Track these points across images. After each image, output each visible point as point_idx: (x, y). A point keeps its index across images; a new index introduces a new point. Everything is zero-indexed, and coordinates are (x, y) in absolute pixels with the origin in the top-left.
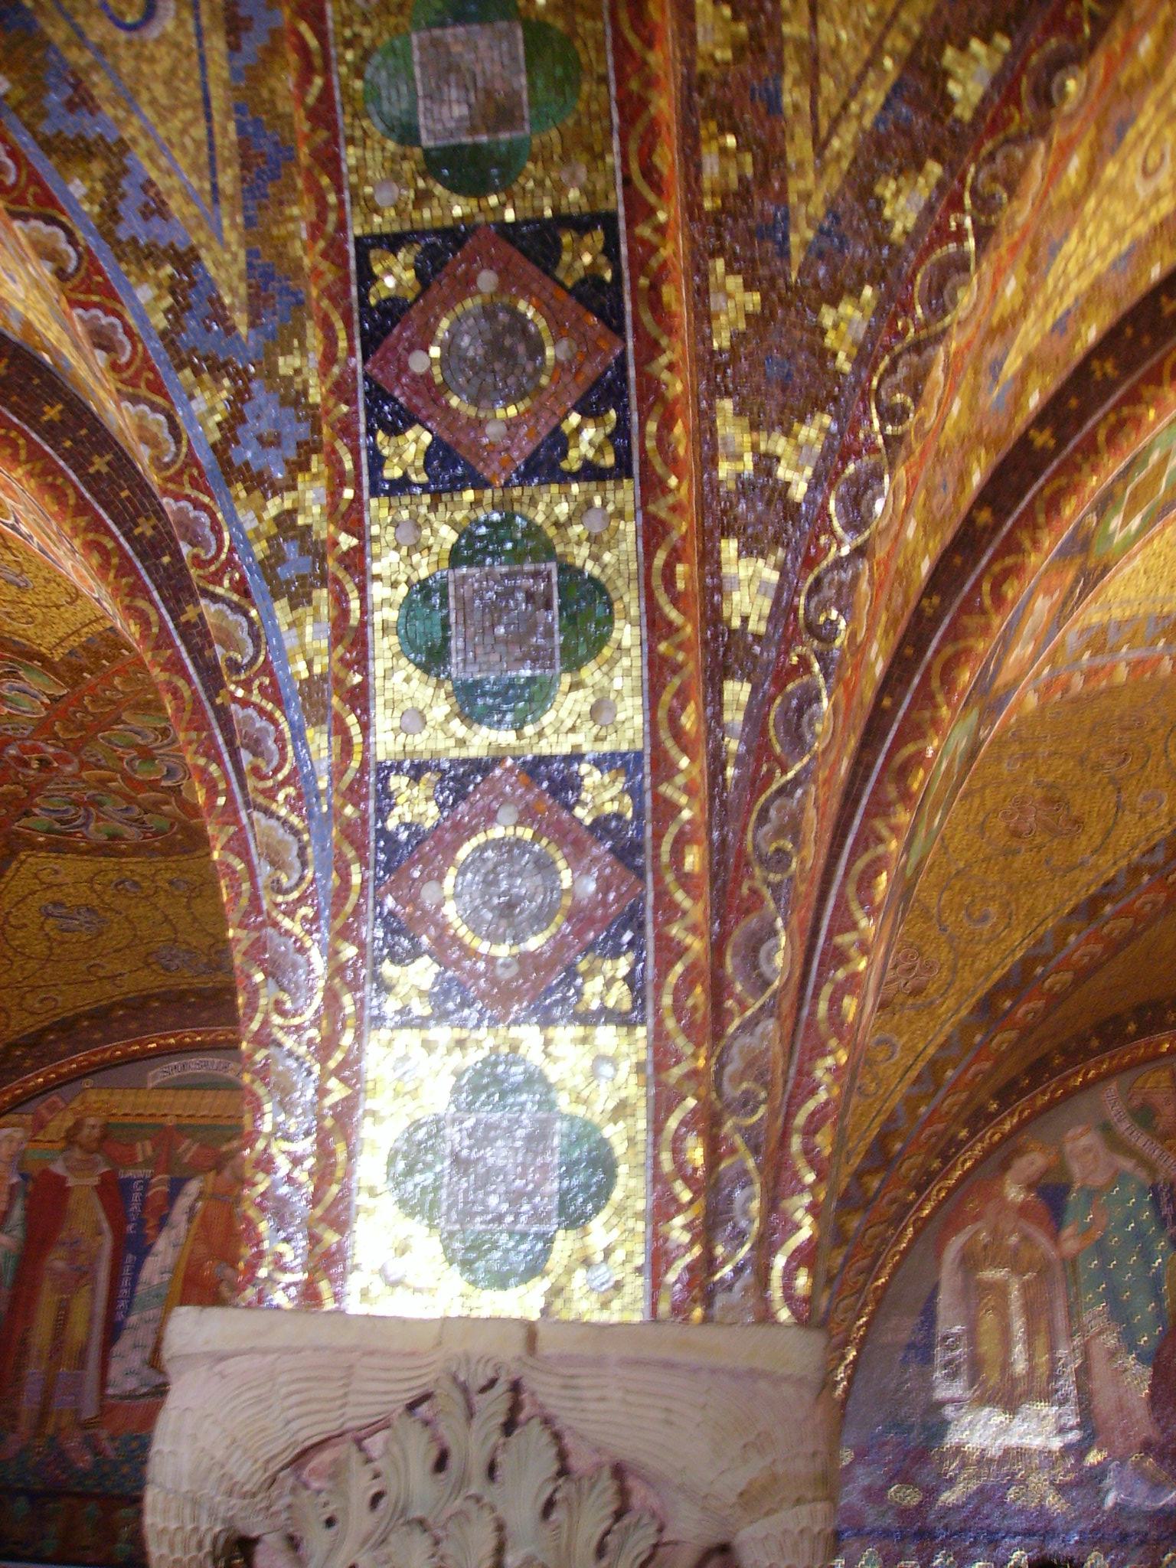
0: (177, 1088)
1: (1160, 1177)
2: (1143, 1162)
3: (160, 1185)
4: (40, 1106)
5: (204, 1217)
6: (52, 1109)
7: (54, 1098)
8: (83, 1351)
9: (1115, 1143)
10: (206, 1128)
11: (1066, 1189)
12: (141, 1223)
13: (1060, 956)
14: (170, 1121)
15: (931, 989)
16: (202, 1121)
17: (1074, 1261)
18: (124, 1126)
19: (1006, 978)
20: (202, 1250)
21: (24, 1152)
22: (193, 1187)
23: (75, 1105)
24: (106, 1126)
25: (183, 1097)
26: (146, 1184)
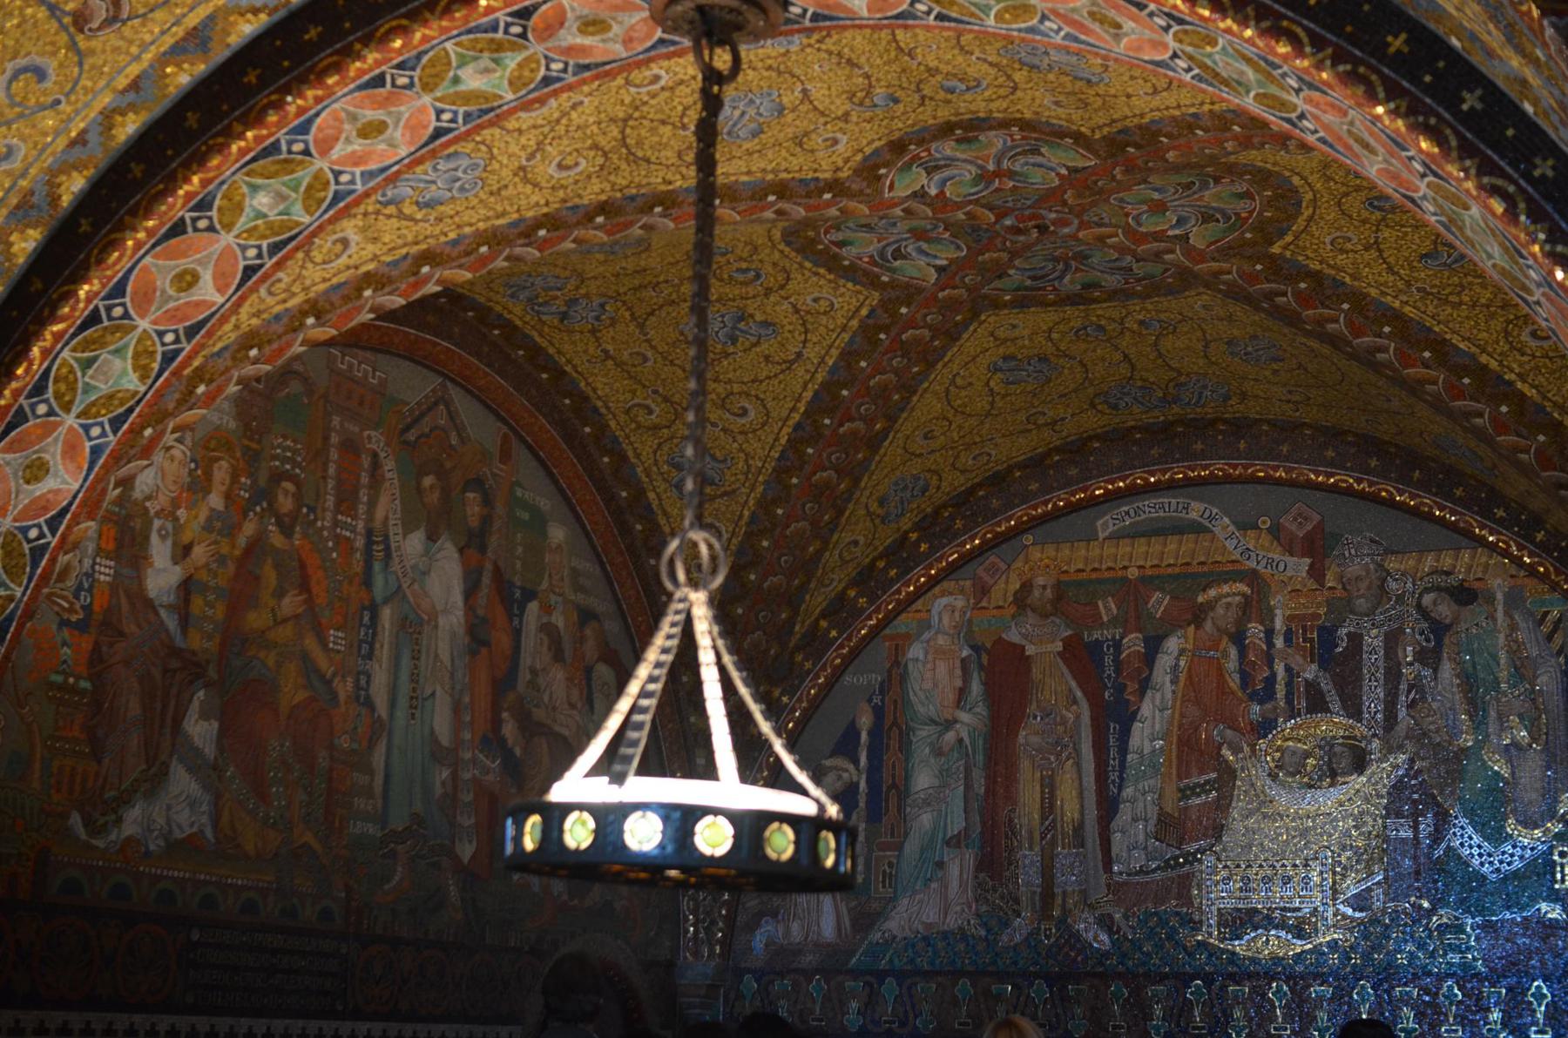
3: (1133, 643)
5: (1190, 677)
7: (993, 558)
8: (1079, 828)
10: (1176, 577)
12: (1120, 689)
14: (1133, 573)
16: (1170, 570)
18: (1080, 584)
21: (970, 621)
22: (1172, 644)
23: (1019, 564)
24: (1058, 586)
25: (1141, 546)
26: (1117, 645)
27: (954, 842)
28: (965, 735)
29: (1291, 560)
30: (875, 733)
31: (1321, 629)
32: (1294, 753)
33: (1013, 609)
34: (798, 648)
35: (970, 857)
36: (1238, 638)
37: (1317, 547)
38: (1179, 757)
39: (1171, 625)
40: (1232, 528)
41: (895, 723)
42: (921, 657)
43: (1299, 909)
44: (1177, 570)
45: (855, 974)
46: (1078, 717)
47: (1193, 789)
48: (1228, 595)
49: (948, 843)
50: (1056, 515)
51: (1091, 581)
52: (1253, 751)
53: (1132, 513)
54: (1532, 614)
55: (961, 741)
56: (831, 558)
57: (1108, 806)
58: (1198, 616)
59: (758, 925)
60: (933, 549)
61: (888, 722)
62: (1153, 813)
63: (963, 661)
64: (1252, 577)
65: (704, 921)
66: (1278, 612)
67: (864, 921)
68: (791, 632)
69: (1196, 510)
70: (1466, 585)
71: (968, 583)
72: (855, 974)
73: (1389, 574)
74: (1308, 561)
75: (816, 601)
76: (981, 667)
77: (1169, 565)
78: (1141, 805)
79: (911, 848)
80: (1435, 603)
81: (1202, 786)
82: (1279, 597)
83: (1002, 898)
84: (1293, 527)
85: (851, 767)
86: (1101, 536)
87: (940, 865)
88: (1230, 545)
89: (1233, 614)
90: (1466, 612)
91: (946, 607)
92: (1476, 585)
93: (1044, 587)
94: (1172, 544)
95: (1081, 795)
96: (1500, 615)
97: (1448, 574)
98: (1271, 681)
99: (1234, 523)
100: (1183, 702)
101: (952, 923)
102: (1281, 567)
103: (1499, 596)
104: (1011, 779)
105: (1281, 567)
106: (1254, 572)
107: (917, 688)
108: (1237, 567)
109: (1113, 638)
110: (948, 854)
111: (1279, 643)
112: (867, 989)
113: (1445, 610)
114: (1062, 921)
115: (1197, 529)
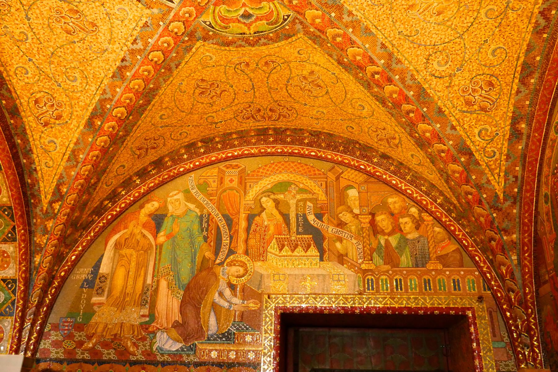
1: (205, 211)
2: (200, 206)
9: (190, 198)
11: (165, 216)
13: (116, 99)
15: (65, 115)
17: (161, 246)
19: (95, 109)
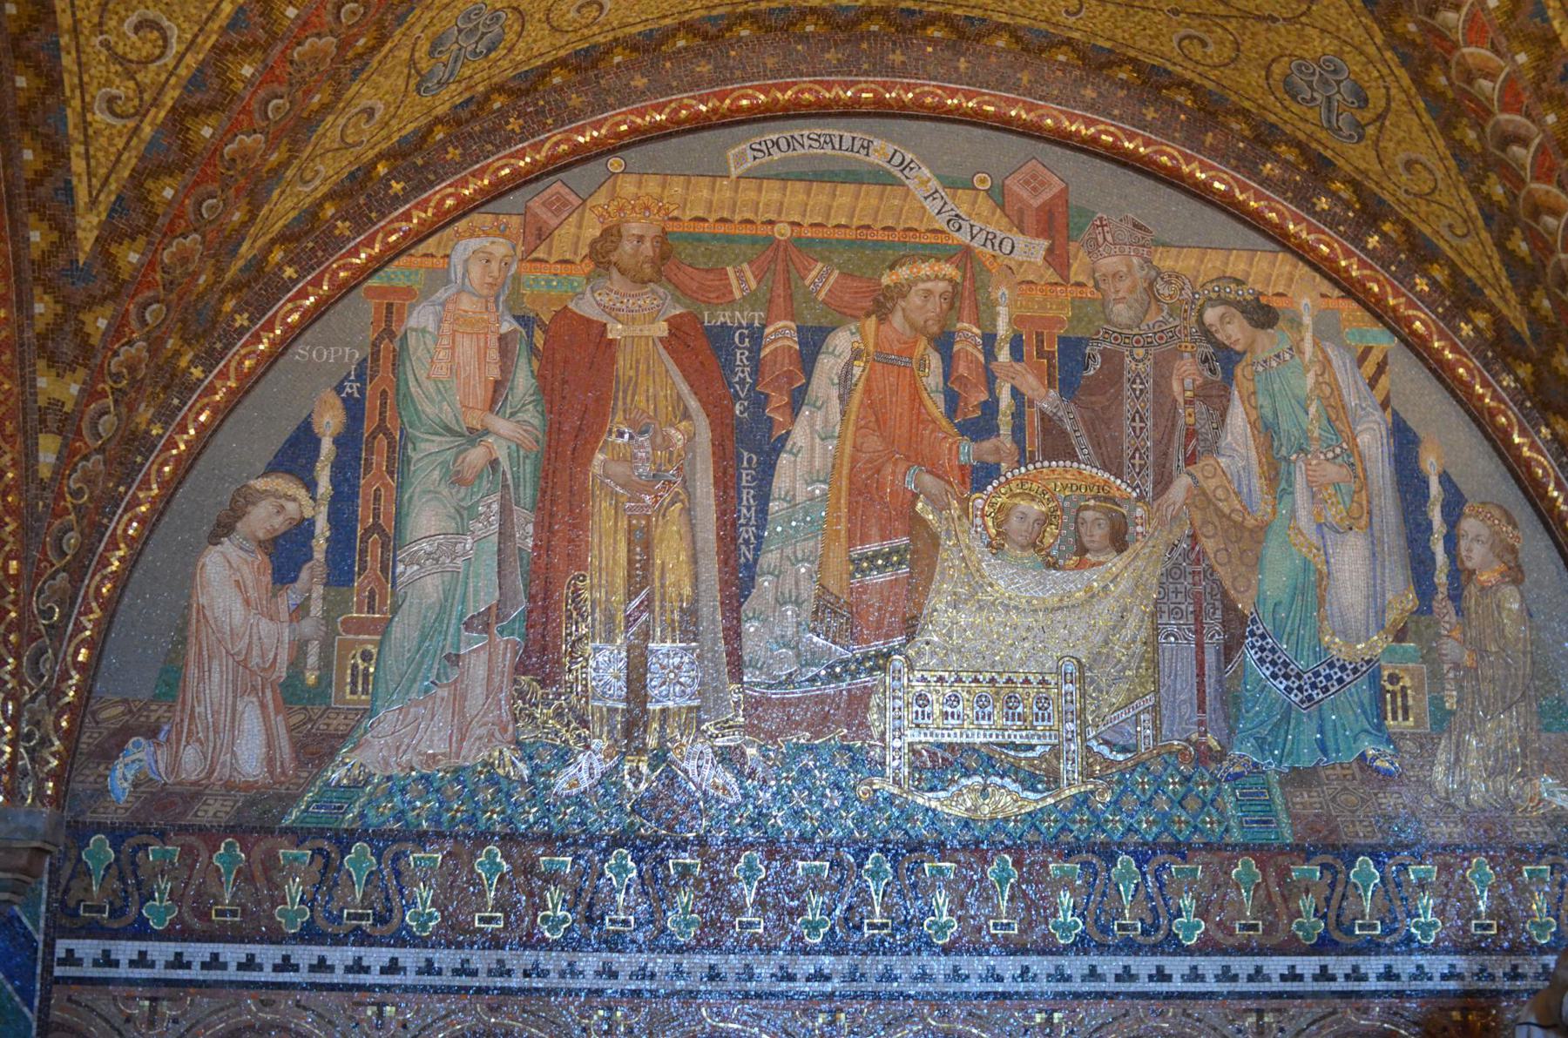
0: (784, 178)
3: (782, 335)
4: (536, 200)
5: (868, 391)
6: (558, 206)
7: (558, 186)
14: (783, 231)
16: (840, 234)
18: (698, 239)
20: (874, 443)
21: (517, 279)
22: (842, 342)
23: (601, 198)
25: (796, 193)
26: (756, 336)
27: (484, 622)
28: (502, 455)
29: (1021, 241)
30: (348, 442)
31: (1063, 340)
32: (1024, 517)
33: (589, 266)
34: (235, 287)
35: (507, 645)
36: (944, 343)
37: (1056, 224)
38: (852, 511)
39: (844, 314)
40: (934, 183)
41: (381, 428)
42: (431, 327)
43: (1032, 747)
44: (850, 235)
45: (299, 835)
46: (691, 438)
47: (871, 559)
48: (928, 279)
49: (468, 626)
50: (660, 134)
51: (714, 237)
52: (965, 512)
53: (783, 143)
54: (1348, 348)
55: (494, 464)
56: (331, 128)
57: (738, 582)
58: (882, 304)
59: (121, 747)
60: (468, 158)
61: (368, 427)
62: (809, 591)
63: (502, 338)
64: (964, 256)
65: (29, 737)
66: (1003, 311)
67: (316, 749)
68: (234, 252)
69: (881, 151)
70: (1263, 300)
71: (515, 221)
72: (299, 835)
73: (1159, 274)
74: (1046, 243)
75: (283, 208)
76: (533, 349)
77: (838, 226)
78: (790, 581)
79: (403, 630)
80: (1222, 317)
81: (887, 557)
82: (1004, 289)
83: (559, 714)
84: (1025, 194)
85: (302, 494)
86: (734, 172)
87: (454, 659)
88: (932, 207)
89: (935, 307)
90: (1263, 336)
91: (477, 252)
92: (1276, 303)
93: (641, 239)
94: (845, 195)
95: (694, 560)
96: (1308, 346)
97: (1239, 282)
98: (990, 408)
99: (938, 177)
100: (858, 429)
101: (472, 755)
102: (1007, 248)
103: (1307, 320)
104: (579, 522)
105: (1007, 248)
106: (967, 251)
107: (422, 375)
108: (941, 239)
109: (750, 326)
110: (472, 644)
111: (1004, 355)
112: (320, 861)
113: (1235, 331)
114: (660, 758)
115: (882, 179)
